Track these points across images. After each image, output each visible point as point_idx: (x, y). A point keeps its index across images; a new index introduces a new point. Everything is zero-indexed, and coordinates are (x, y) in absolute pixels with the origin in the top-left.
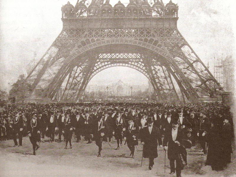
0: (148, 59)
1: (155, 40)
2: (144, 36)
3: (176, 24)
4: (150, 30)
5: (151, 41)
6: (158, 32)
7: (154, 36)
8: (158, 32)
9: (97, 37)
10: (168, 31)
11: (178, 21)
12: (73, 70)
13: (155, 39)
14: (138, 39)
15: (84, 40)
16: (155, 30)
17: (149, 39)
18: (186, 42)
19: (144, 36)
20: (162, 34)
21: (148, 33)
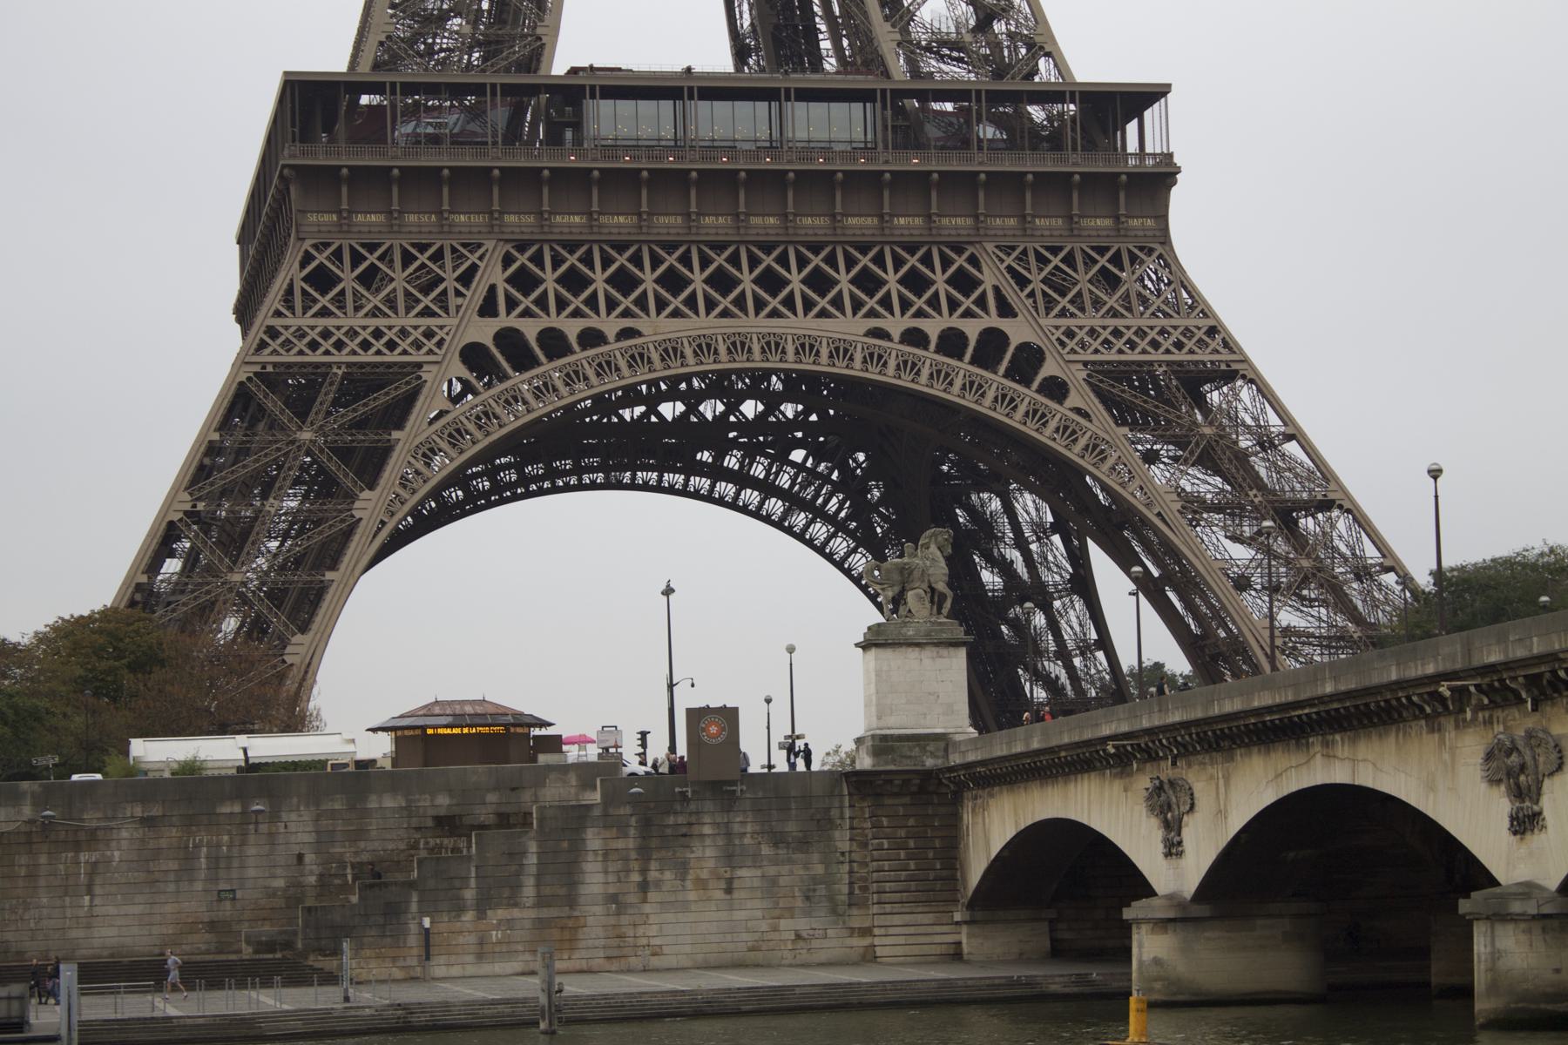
0: (894, 479)
1: (1015, 342)
2: (934, 302)
3: (1163, 218)
4: (973, 260)
5: (991, 347)
6: (1036, 279)
7: (1006, 310)
8: (1037, 284)
9: (577, 313)
10: (1103, 270)
11: (1178, 197)
12: (1055, 528)
13: (1018, 331)
14: (896, 336)
15: (483, 332)
16: (1009, 261)
17: (972, 329)
18: (1245, 360)
19: (934, 302)
20: (1063, 295)
21: (965, 282)
